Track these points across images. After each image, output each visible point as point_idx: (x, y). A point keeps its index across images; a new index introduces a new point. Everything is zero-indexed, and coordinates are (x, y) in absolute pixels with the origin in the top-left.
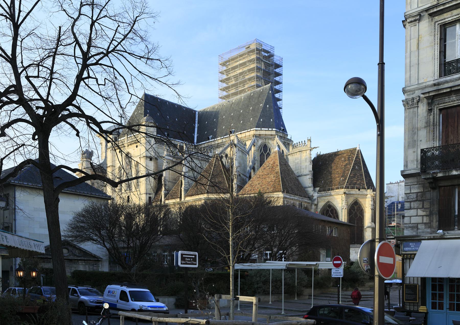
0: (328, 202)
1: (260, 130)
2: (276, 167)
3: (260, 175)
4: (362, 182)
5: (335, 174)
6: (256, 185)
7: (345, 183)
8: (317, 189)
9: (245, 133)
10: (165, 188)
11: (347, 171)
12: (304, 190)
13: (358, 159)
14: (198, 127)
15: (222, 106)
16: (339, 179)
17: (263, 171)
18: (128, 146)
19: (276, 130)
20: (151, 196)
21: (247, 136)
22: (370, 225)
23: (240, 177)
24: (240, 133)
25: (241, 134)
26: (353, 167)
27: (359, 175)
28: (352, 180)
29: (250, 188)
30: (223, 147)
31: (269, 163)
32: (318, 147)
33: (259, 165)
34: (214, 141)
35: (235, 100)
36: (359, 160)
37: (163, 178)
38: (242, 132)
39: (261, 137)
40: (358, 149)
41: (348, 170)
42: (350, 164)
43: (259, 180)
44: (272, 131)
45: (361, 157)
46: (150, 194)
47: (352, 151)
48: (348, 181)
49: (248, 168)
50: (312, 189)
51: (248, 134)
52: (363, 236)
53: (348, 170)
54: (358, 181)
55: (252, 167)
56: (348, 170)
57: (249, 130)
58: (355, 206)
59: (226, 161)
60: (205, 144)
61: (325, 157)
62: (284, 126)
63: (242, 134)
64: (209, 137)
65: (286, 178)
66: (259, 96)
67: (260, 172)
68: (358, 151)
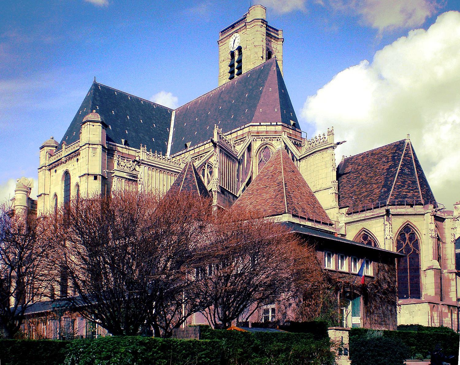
0: (364, 230)
1: (259, 125)
2: (278, 176)
4: (416, 194)
5: (372, 184)
6: (247, 205)
7: (388, 197)
8: (344, 210)
11: (390, 177)
12: (324, 212)
13: (408, 157)
16: (380, 191)
17: (258, 184)
19: (282, 125)
22: (430, 264)
26: (400, 169)
27: (410, 182)
28: (401, 191)
31: (268, 171)
32: (345, 142)
35: (226, 88)
36: (409, 159)
38: (233, 131)
40: (407, 141)
41: (392, 176)
42: (396, 166)
44: (277, 127)
45: (412, 155)
47: (397, 146)
48: (393, 192)
50: (337, 210)
52: (420, 285)
53: (392, 176)
54: (409, 192)
56: (394, 176)
57: (243, 127)
58: (406, 234)
61: (357, 159)
62: (295, 119)
65: (294, 192)
68: (408, 144)
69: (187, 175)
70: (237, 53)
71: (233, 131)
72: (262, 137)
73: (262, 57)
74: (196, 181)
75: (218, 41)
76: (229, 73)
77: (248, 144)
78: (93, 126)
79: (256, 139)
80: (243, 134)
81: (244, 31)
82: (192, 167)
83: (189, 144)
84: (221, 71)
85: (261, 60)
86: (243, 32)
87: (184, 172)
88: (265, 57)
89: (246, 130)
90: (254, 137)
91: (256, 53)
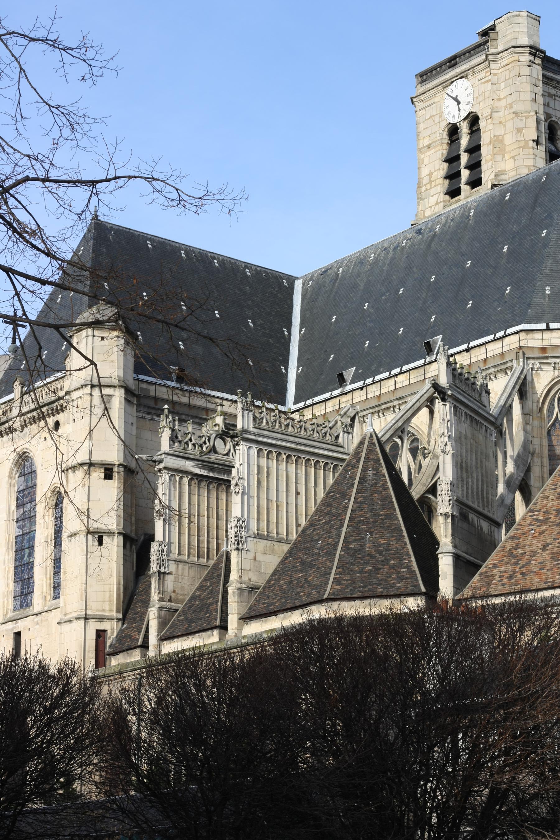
3: (547, 512)
6: (534, 553)
9: (483, 349)
10: (162, 591)
14: (303, 340)
15: (395, 249)
18: (24, 426)
20: (105, 625)
21: (493, 356)
23: (465, 525)
24: (464, 347)
25: (467, 350)
29: (508, 567)
30: (397, 410)
33: (546, 470)
34: (361, 389)
35: (444, 225)
37: (154, 547)
38: (472, 344)
39: (547, 358)
43: (543, 532)
46: (101, 619)
49: (501, 488)
51: (494, 349)
55: (517, 483)
57: (501, 334)
59: (413, 466)
60: (329, 403)
63: (472, 351)
64: (344, 373)
66: (535, 202)
67: (546, 498)
69: (365, 469)
70: (464, 128)
71: (472, 344)
72: (554, 360)
73: (537, 142)
74: (389, 484)
75: (412, 99)
76: (446, 178)
77: (520, 381)
78: (103, 338)
79: (538, 365)
80: (502, 354)
81: (483, 74)
82: (378, 449)
83: (349, 373)
84: (424, 172)
85: (533, 148)
86: (479, 77)
87: (354, 461)
88: (543, 140)
89: (512, 342)
90: (532, 361)
91: (519, 130)
